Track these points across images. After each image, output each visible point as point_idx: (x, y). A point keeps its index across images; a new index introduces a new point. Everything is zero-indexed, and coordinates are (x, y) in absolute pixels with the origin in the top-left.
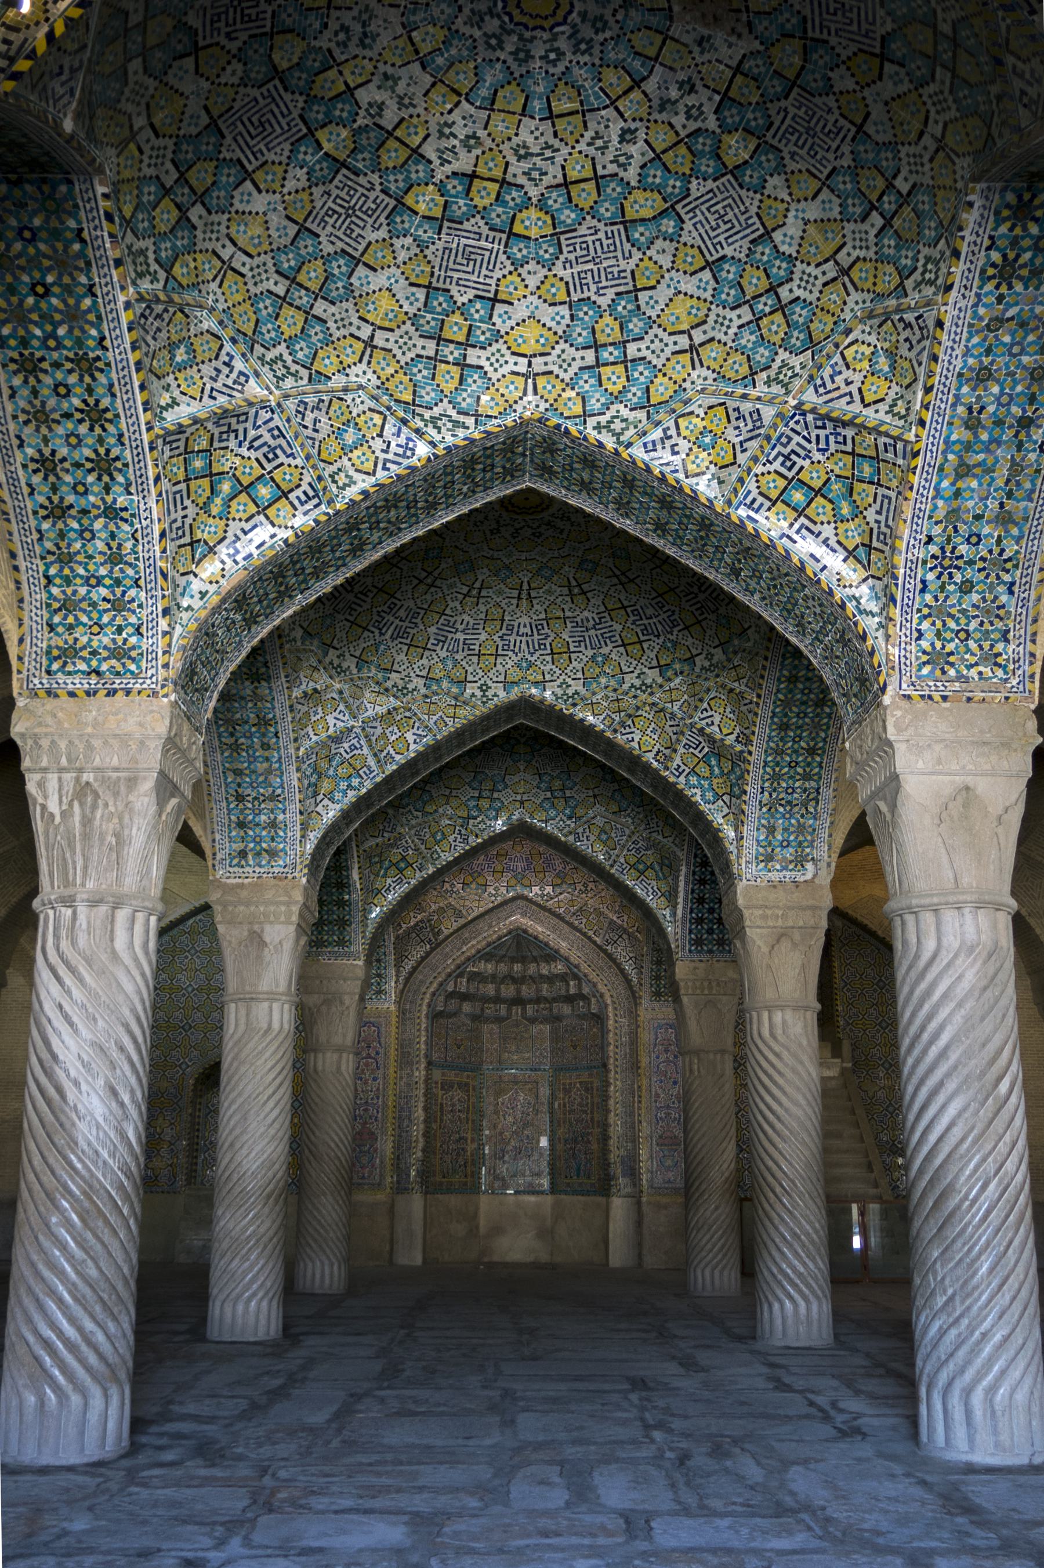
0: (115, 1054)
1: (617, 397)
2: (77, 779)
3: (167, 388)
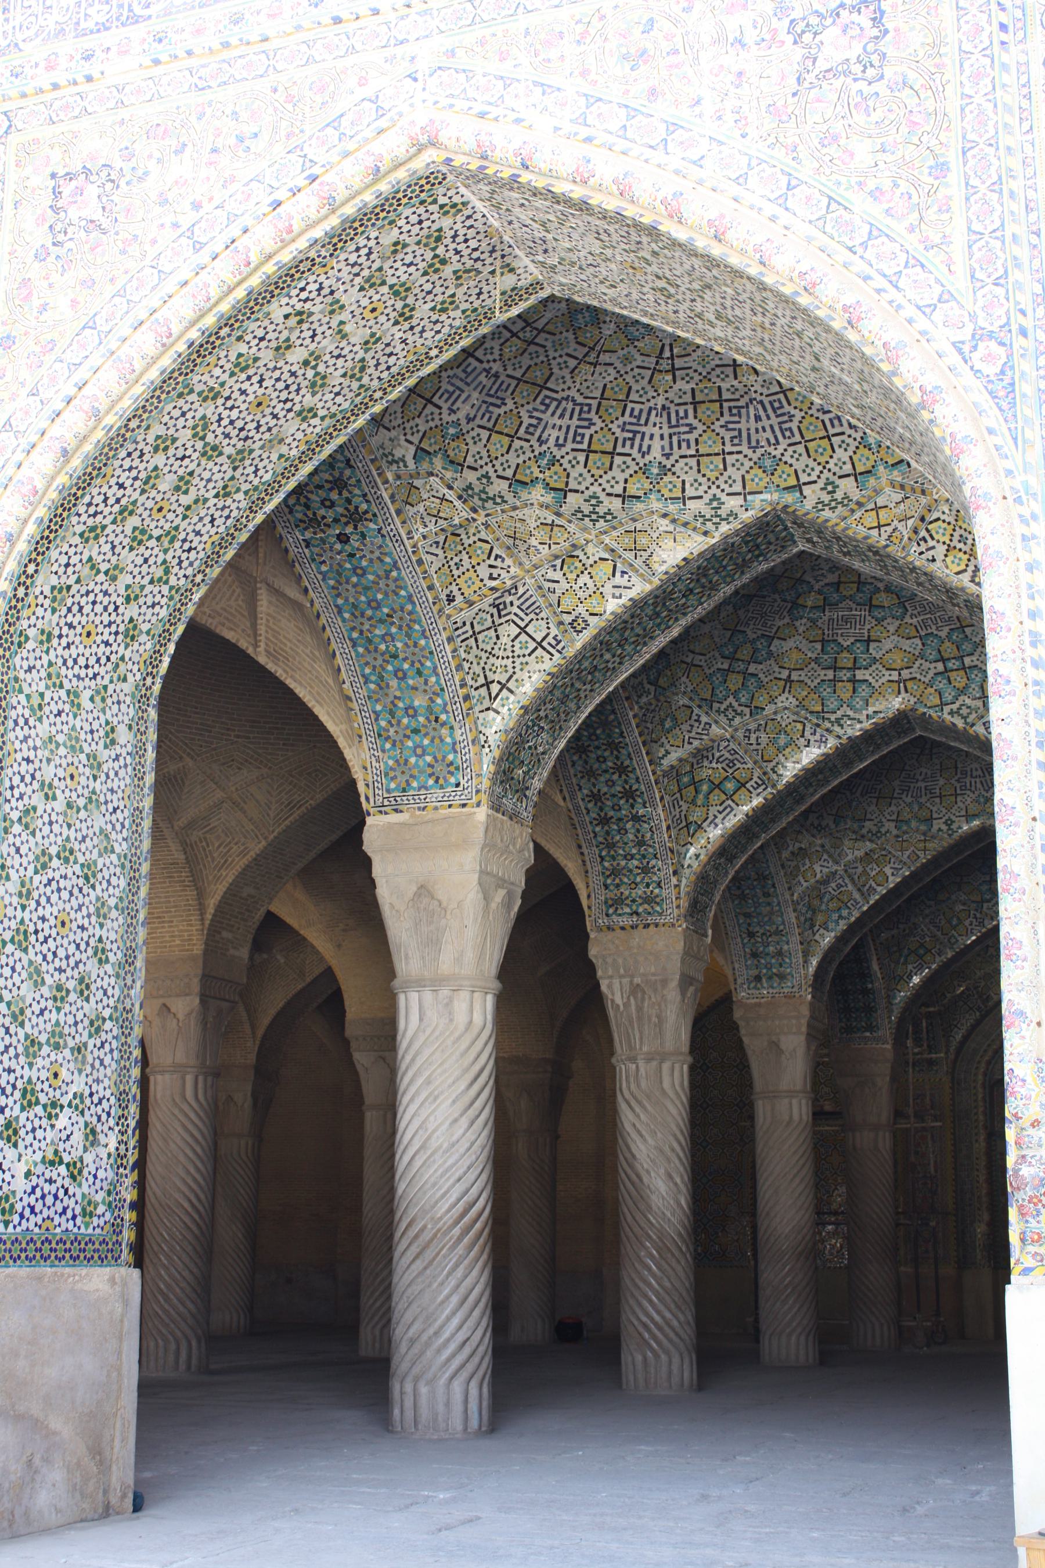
0: (669, 1153)
1: (963, 691)
2: (631, 982)
3: (662, 745)
